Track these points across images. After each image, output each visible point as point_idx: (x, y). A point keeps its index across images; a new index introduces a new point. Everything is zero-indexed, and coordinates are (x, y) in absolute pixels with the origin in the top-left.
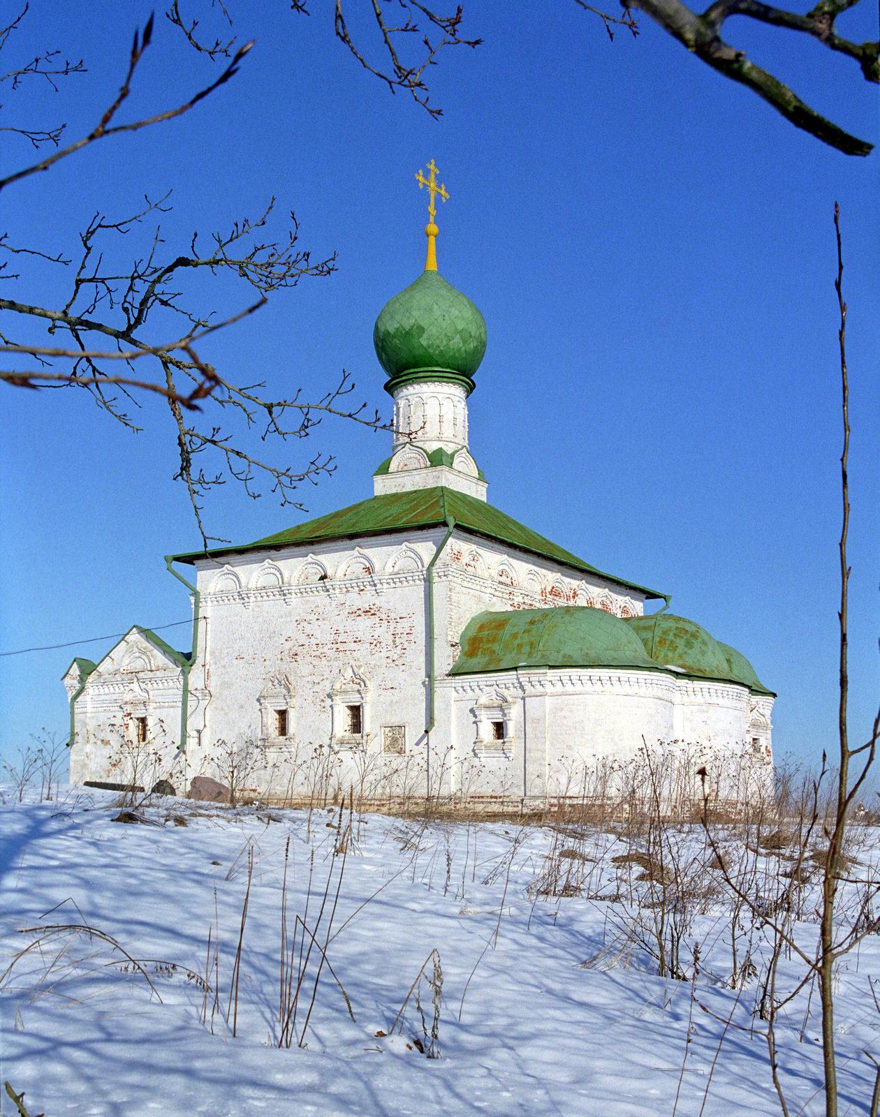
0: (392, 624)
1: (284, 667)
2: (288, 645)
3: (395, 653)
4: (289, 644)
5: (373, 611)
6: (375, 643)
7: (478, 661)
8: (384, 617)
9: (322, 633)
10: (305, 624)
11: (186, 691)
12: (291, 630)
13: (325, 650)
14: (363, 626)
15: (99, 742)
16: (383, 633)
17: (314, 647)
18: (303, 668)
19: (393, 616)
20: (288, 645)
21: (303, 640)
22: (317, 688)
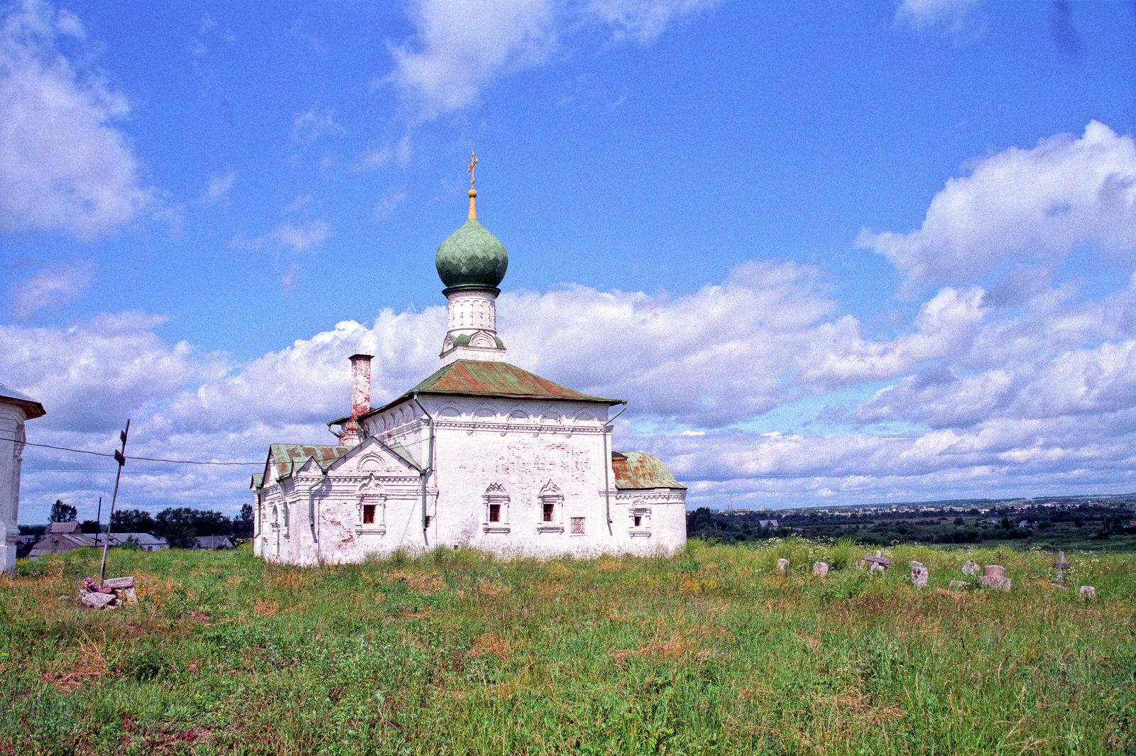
0: (575, 456)
1: (499, 477)
2: (503, 462)
3: (578, 474)
4: (503, 462)
5: (562, 447)
6: (565, 466)
8: (570, 451)
9: (527, 457)
12: (505, 453)
14: (556, 455)
15: (330, 523)
16: (570, 460)
17: (522, 465)
18: (514, 477)
19: (575, 451)
21: (515, 460)
22: (524, 491)
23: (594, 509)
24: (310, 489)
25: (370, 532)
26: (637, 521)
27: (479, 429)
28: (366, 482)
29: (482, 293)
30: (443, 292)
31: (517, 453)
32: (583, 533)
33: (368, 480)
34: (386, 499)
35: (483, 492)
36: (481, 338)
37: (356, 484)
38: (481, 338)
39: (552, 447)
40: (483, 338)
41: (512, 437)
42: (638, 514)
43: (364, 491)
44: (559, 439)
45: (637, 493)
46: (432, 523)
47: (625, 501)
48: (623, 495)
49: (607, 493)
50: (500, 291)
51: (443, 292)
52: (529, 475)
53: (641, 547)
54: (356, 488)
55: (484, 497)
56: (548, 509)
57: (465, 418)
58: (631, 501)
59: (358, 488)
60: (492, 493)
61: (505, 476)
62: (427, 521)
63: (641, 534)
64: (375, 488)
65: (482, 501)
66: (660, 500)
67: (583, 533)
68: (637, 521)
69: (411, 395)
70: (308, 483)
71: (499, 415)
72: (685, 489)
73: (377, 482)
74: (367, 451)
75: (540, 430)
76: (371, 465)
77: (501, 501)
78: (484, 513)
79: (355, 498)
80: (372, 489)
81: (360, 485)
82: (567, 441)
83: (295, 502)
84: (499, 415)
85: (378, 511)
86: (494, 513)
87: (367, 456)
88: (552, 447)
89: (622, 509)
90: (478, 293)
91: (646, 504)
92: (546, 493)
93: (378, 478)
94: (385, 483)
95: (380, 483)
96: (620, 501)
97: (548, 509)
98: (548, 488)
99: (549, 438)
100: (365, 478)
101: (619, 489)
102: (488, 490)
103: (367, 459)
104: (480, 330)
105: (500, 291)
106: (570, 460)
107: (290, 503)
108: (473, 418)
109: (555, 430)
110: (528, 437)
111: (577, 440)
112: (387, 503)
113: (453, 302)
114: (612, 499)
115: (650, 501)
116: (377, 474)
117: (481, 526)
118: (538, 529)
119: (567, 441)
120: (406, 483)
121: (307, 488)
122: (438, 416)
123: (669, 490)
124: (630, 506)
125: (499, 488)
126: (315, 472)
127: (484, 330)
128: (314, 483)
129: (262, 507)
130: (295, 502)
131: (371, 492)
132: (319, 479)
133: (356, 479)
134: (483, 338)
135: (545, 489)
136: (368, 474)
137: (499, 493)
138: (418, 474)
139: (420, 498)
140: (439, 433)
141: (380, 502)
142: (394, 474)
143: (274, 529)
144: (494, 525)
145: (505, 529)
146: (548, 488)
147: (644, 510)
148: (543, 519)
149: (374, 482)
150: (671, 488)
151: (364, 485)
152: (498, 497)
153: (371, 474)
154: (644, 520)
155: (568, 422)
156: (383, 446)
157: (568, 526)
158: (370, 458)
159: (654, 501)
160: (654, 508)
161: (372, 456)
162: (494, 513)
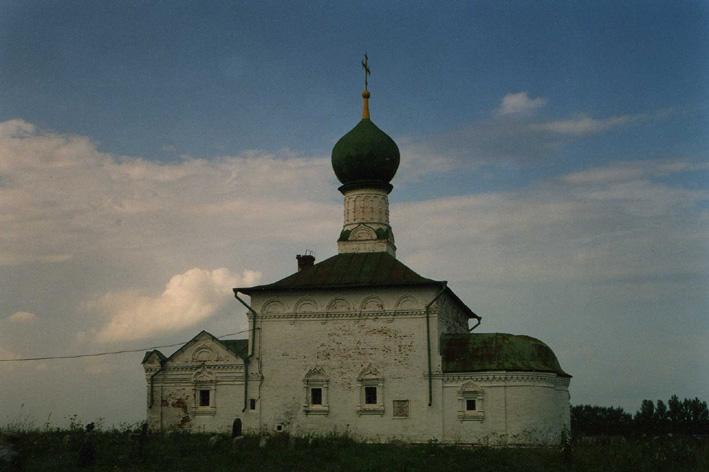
1: (320, 362)
2: (324, 348)
4: (324, 348)
6: (387, 350)
7: (452, 365)
10: (335, 337)
11: (247, 374)
13: (350, 352)
14: (378, 340)
16: (391, 344)
18: (334, 362)
20: (322, 349)
21: (334, 345)
23: (416, 391)
25: (203, 413)
26: (471, 405)
28: (199, 370)
30: (340, 189)
31: (337, 339)
32: (407, 416)
34: (216, 385)
39: (374, 331)
41: (330, 326)
43: (199, 378)
44: (380, 324)
46: (257, 405)
47: (453, 384)
49: (430, 376)
51: (340, 189)
52: (349, 360)
53: (471, 433)
54: (192, 375)
55: (304, 381)
56: (371, 395)
58: (460, 384)
61: (327, 361)
63: (374, 412)
66: (495, 384)
67: (407, 416)
68: (471, 405)
76: (203, 356)
78: (303, 396)
80: (206, 377)
82: (390, 326)
85: (211, 394)
86: (316, 396)
88: (374, 331)
89: (451, 391)
92: (368, 377)
93: (209, 367)
97: (371, 395)
99: (370, 324)
102: (308, 375)
106: (391, 344)
108: (296, 308)
109: (376, 316)
110: (352, 325)
111: (401, 325)
112: (218, 387)
114: (438, 383)
117: (302, 409)
118: (358, 412)
119: (390, 326)
120: (233, 371)
131: (205, 379)
136: (199, 364)
137: (320, 378)
141: (213, 387)
142: (222, 363)
145: (325, 411)
147: (475, 392)
148: (310, 400)
152: (318, 381)
154: (478, 405)
155: (390, 307)
157: (390, 410)
160: (487, 390)
162: (316, 396)
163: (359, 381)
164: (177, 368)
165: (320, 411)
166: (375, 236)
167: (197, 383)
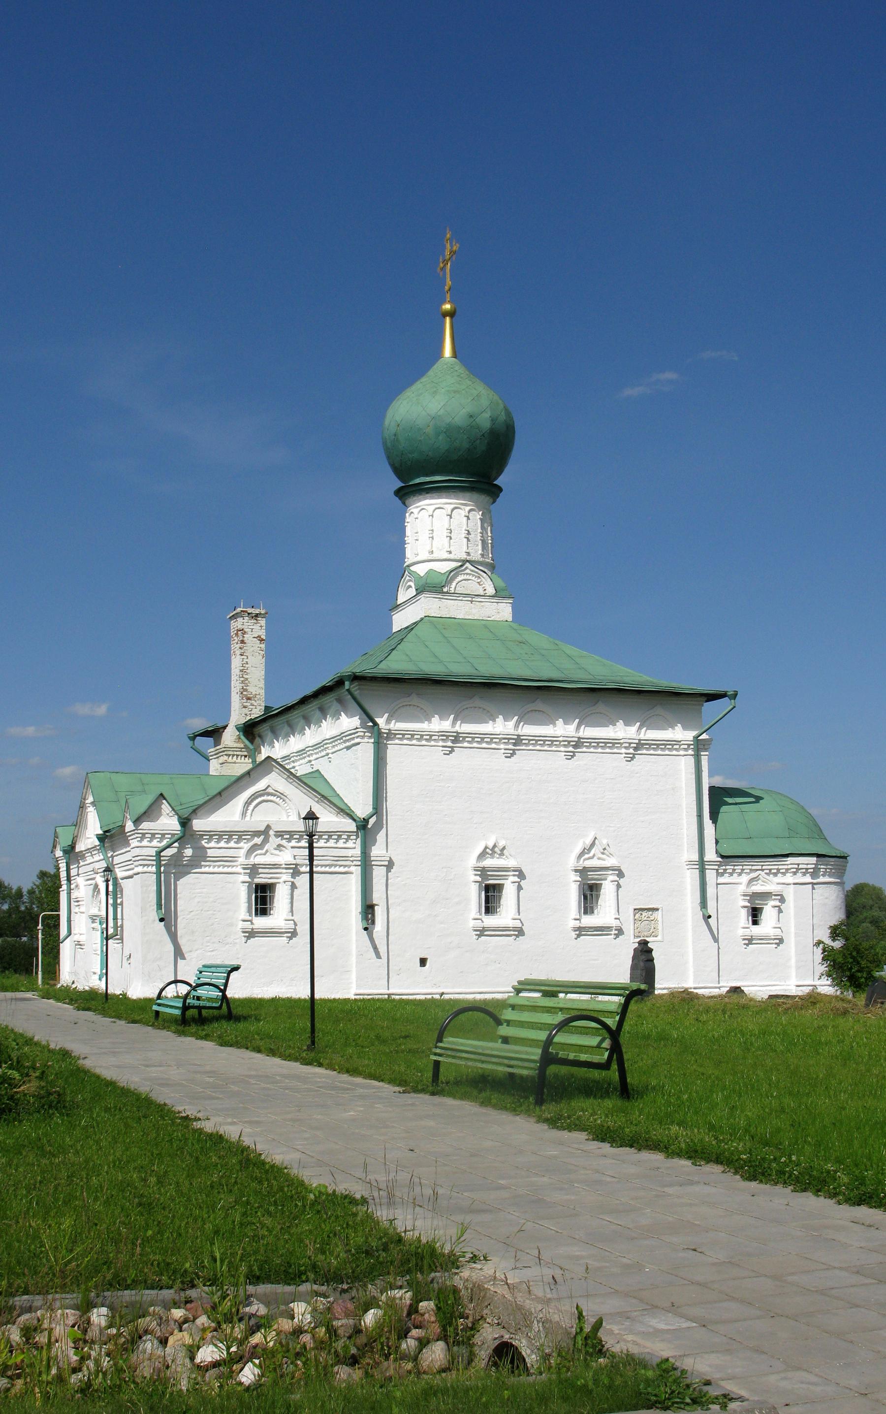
24: (159, 853)
26: (755, 915)
27: (466, 744)
28: (258, 840)
29: (468, 495)
33: (262, 837)
35: (472, 861)
36: (465, 577)
37: (241, 844)
38: (465, 577)
40: (470, 577)
42: (758, 903)
43: (258, 859)
45: (757, 864)
47: (735, 878)
48: (729, 868)
49: (702, 865)
50: (500, 489)
57: (438, 724)
58: (745, 879)
59: (242, 853)
60: (488, 862)
62: (368, 910)
64: (277, 852)
65: (473, 877)
68: (755, 915)
69: (339, 683)
70: (155, 843)
71: (620, 724)
72: (845, 857)
73: (279, 841)
74: (261, 785)
75: (575, 747)
77: (505, 877)
78: (474, 896)
79: (239, 869)
81: (245, 846)
83: (131, 877)
84: (620, 724)
87: (264, 792)
90: (461, 494)
91: (769, 884)
92: (589, 864)
93: (280, 834)
94: (293, 843)
95: (284, 842)
96: (725, 879)
98: (591, 854)
100: (257, 834)
101: (722, 857)
102: (483, 855)
103: (260, 799)
104: (465, 562)
105: (500, 489)
107: (123, 879)
113: (415, 511)
114: (711, 875)
115: (780, 879)
116: (276, 828)
121: (153, 852)
122: (388, 721)
123: (813, 860)
124: (742, 888)
125: (502, 854)
126: (168, 822)
127: (471, 562)
128: (165, 842)
129: (72, 887)
130: (131, 877)
132: (173, 835)
133: (240, 836)
134: (470, 577)
135: (586, 856)
138: (352, 826)
139: (357, 871)
140: (394, 752)
143: (94, 925)
144: (490, 921)
146: (591, 854)
149: (274, 841)
150: (818, 856)
151: (255, 848)
153: (268, 827)
154: (768, 913)
156: (291, 776)
158: (265, 798)
159: (789, 878)
160: (790, 893)
161: (269, 794)
163: (576, 871)
164: (220, 835)
165: (506, 929)
166: (491, 591)
167: (253, 870)
